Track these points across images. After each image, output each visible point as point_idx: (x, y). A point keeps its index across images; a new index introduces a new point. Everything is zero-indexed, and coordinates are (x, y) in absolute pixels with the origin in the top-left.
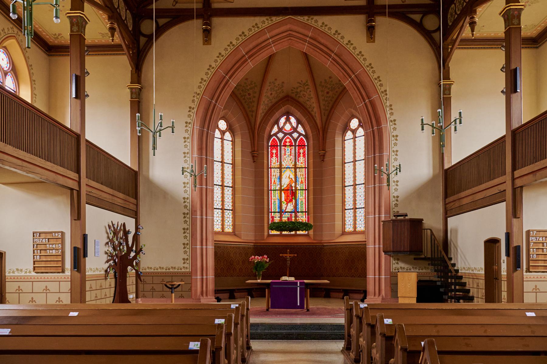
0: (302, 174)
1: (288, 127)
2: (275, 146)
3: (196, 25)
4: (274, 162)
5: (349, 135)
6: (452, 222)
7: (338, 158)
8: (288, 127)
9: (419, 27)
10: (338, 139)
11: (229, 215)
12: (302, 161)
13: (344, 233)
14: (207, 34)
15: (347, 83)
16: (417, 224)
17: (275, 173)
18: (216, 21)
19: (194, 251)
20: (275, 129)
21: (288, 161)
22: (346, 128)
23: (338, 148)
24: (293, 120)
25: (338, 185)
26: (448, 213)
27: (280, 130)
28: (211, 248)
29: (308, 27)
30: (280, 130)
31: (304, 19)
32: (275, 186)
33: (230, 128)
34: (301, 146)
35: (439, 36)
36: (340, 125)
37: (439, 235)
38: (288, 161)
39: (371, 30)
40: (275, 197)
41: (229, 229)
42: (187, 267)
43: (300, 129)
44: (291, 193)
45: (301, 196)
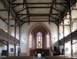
0: (41, 40)
1: (39, 34)
2: (37, 36)
3: (27, 23)
4: (37, 38)
5: (48, 35)
6: (60, 46)
7: (46, 38)
8: (39, 34)
9: (55, 23)
10: (46, 35)
11: (31, 45)
12: (41, 38)
13: (47, 48)
14: (29, 24)
15: (47, 30)
16: (56, 47)
17: (37, 40)
18: (30, 22)
19: (27, 50)
20: (38, 34)
21: (39, 38)
22: (47, 34)
23: (46, 37)
24: (40, 33)
25: (46, 42)
26: (59, 45)
27: (38, 34)
28: (29, 50)
29: (42, 23)
30: (38, 34)
31: (41, 22)
32: (37, 41)
33: (31, 34)
34: (41, 36)
35: (58, 24)
36: (46, 34)
37: (58, 48)
38: (39, 38)
39: (49, 24)
40: (37, 43)
41: (31, 47)
42: (26, 52)
43: (41, 34)
44: (40, 43)
45: (41, 43)
